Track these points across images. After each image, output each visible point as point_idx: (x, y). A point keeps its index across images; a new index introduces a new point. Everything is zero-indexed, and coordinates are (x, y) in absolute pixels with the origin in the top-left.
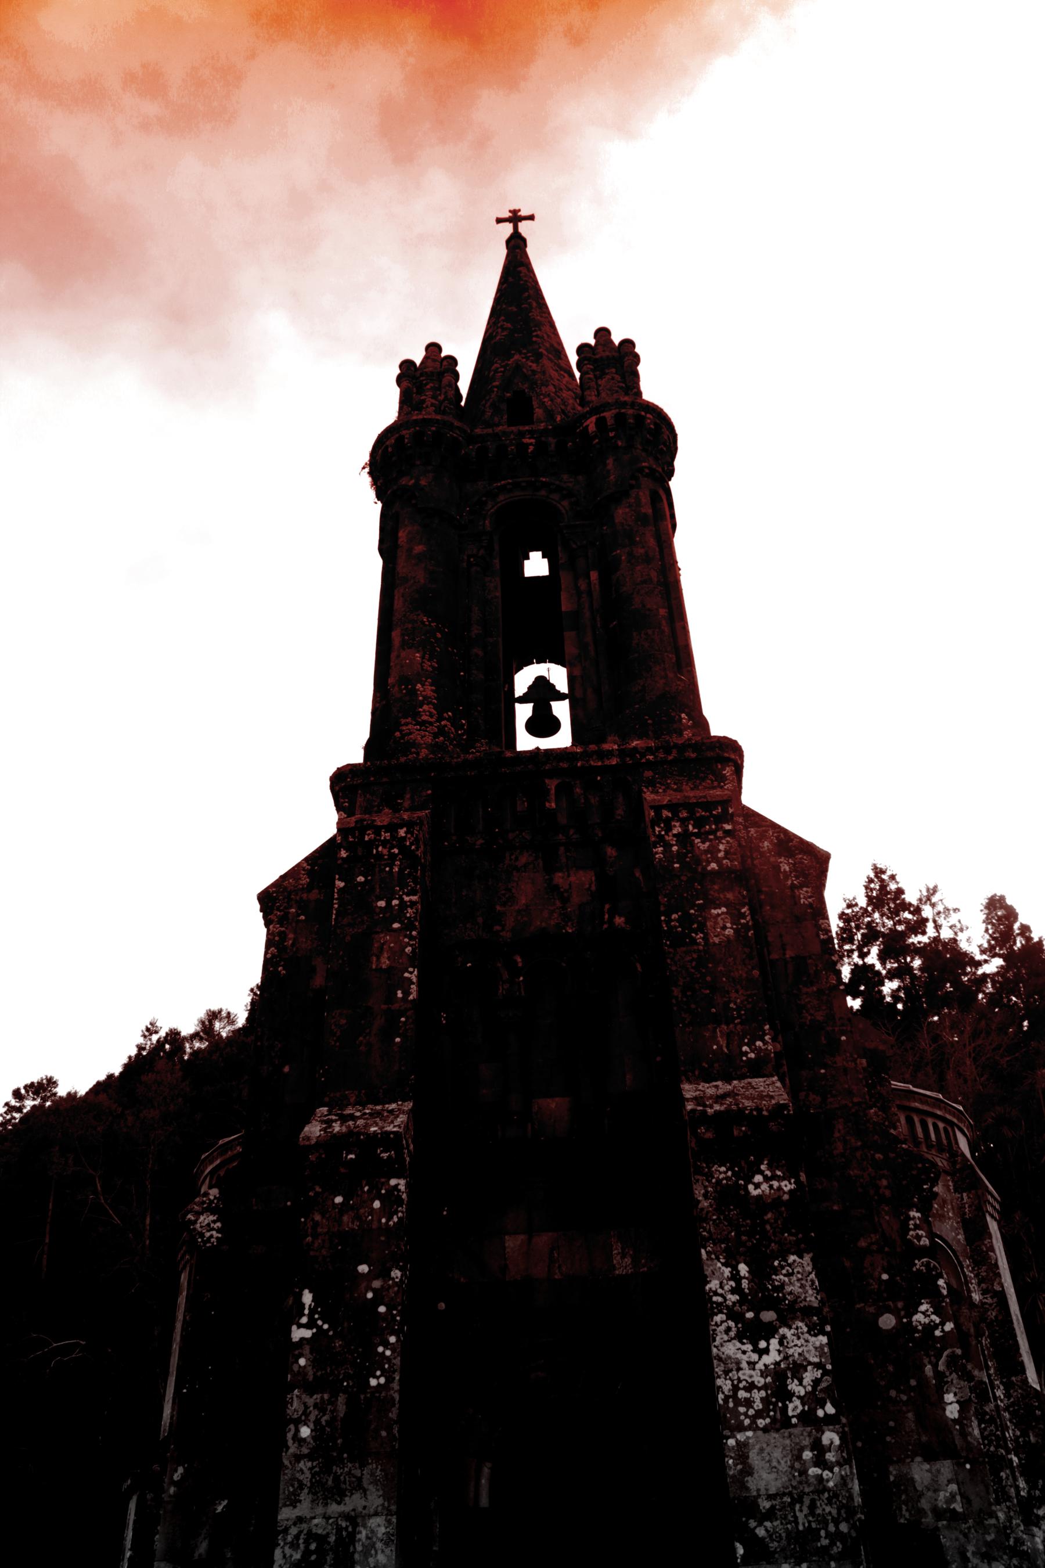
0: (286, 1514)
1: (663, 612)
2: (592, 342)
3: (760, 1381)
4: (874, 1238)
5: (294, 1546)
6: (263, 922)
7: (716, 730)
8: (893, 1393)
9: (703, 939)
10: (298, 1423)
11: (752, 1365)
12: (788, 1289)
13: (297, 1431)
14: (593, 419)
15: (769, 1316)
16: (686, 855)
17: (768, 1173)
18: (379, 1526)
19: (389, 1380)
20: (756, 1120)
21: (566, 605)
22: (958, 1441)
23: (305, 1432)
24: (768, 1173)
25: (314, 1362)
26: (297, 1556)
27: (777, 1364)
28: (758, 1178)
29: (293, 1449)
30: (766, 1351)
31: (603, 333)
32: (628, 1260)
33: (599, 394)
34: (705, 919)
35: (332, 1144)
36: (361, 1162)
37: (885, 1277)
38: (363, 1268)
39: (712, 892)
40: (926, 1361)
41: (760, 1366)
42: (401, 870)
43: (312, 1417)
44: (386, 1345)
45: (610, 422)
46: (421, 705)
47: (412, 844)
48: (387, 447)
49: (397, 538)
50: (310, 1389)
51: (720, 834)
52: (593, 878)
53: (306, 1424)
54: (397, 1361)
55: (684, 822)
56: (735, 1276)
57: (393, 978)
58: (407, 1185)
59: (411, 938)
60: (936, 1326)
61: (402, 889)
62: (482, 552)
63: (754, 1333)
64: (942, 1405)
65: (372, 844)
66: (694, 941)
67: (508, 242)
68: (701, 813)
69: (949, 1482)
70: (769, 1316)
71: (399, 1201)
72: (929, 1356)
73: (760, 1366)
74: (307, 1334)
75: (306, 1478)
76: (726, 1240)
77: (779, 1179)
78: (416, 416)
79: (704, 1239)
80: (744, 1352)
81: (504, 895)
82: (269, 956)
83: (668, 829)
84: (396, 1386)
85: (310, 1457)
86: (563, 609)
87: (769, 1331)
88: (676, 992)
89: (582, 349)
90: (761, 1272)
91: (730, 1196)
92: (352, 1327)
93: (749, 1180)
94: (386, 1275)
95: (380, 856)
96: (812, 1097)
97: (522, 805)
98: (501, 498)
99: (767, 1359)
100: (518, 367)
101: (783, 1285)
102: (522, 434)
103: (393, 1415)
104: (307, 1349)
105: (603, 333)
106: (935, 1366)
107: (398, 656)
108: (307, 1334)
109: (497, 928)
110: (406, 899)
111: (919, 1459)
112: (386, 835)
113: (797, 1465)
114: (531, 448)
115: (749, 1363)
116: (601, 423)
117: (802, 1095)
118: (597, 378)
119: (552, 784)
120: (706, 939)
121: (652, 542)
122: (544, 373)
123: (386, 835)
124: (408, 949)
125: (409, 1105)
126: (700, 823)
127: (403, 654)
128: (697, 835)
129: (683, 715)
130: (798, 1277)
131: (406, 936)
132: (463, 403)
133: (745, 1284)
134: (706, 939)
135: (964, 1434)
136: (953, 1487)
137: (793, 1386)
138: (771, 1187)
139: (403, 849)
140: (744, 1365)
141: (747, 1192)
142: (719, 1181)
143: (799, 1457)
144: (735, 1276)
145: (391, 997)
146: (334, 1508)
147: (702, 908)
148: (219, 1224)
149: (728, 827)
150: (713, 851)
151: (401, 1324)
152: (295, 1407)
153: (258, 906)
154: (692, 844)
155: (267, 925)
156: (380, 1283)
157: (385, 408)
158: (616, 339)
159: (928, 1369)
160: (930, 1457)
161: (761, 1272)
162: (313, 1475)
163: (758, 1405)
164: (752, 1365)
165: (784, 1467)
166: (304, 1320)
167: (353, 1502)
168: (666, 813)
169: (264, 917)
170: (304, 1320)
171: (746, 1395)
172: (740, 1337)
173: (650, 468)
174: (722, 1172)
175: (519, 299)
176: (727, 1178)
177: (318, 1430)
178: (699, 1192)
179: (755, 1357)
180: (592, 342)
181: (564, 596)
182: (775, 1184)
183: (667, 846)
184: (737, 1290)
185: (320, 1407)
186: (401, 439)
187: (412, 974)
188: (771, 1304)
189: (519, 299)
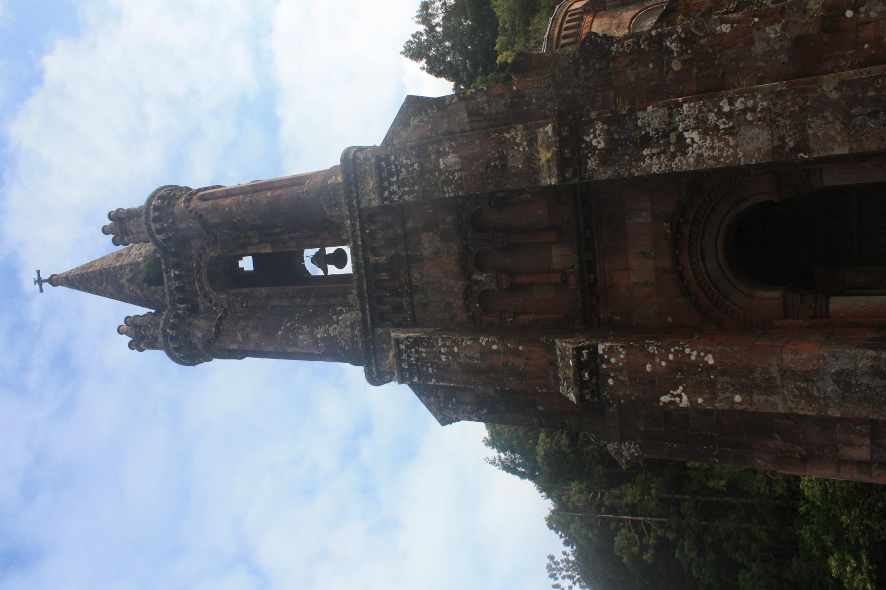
1: (269, 194)
2: (111, 236)
3: (708, 143)
4: (628, 72)
7: (338, 162)
10: (733, 403)
11: (700, 148)
12: (657, 125)
13: (737, 403)
15: (673, 137)
16: (410, 183)
17: (592, 136)
19: (710, 352)
20: (562, 143)
21: (267, 250)
23: (738, 398)
24: (592, 136)
25: (701, 396)
27: (699, 133)
28: (594, 143)
30: (692, 139)
31: (105, 231)
32: (643, 214)
33: (143, 232)
34: (447, 171)
35: (581, 385)
38: (648, 367)
42: (424, 347)
43: (731, 395)
44: (690, 355)
45: (158, 226)
46: (329, 334)
49: (233, 350)
51: (397, 163)
53: (733, 398)
54: (700, 348)
55: (391, 184)
58: (602, 342)
61: (434, 346)
62: (239, 299)
64: (723, 34)
65: (409, 364)
66: (460, 178)
67: (54, 286)
68: (385, 175)
70: (673, 137)
71: (611, 348)
74: (685, 398)
75: (762, 398)
76: (630, 161)
77: (595, 130)
78: (161, 339)
79: (630, 173)
80: (693, 152)
83: (394, 193)
84: (713, 349)
87: (681, 138)
89: (115, 242)
91: (605, 157)
92: (683, 372)
93: (596, 148)
96: (549, 107)
97: (384, 275)
98: (207, 289)
99: (697, 139)
100: (129, 280)
102: (169, 278)
103: (729, 350)
105: (105, 231)
106: (701, 37)
108: (685, 398)
110: (440, 344)
111: (753, 48)
112: (405, 356)
113: (755, 123)
114: (177, 272)
116: (159, 231)
117: (548, 113)
118: (132, 234)
119: (373, 259)
120: (458, 171)
121: (228, 201)
122: (131, 264)
123: (405, 356)
124: (468, 342)
125: (558, 342)
126: (391, 174)
127: (301, 345)
128: (398, 176)
130: (652, 117)
132: (153, 311)
133: (655, 151)
134: (458, 171)
135: (739, 22)
138: (599, 135)
140: (700, 152)
142: (597, 165)
143: (751, 122)
145: (497, 352)
147: (441, 172)
148: (627, 443)
149: (393, 158)
150: (406, 166)
151: (679, 346)
153: (448, 426)
154: (403, 179)
155: (459, 421)
157: (157, 357)
158: (109, 222)
160: (752, 43)
161: (646, 141)
162: (761, 394)
163: (722, 144)
164: (700, 148)
165: (756, 130)
166: (677, 399)
170: (677, 399)
171: (717, 151)
172: (684, 154)
173: (185, 202)
174: (591, 164)
175: (88, 280)
176: (595, 159)
178: (603, 177)
180: (111, 236)
181: (263, 251)
182: (598, 132)
183: (405, 193)
184: (658, 155)
185: (725, 390)
186: (175, 348)
187: (483, 340)
188: (666, 135)
189: (88, 280)
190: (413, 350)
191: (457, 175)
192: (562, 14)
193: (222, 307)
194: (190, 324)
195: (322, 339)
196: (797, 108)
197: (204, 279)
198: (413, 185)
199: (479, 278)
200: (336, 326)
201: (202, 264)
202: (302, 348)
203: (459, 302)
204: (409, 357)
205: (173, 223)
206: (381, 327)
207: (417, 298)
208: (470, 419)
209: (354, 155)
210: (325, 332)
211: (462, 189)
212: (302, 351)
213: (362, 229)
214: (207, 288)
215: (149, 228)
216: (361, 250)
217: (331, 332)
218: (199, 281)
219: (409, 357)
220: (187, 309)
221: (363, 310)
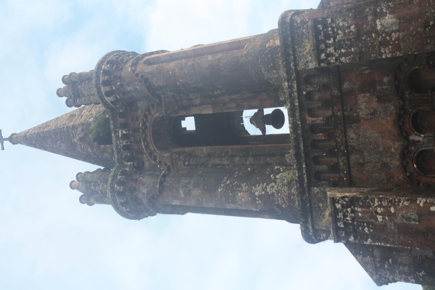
1: (210, 58)
2: (65, 98)
6: (393, 284)
7: (275, 26)
9: (395, 33)
14: (106, 98)
16: (346, 45)
21: (208, 111)
31: (60, 93)
33: (93, 95)
34: (384, 32)
39: (368, 29)
42: (360, 207)
45: (107, 89)
46: (266, 192)
48: (127, 211)
49: (176, 206)
51: (334, 25)
52: (362, 95)
55: (327, 46)
59: (399, 201)
61: (370, 206)
62: (182, 157)
65: (345, 224)
66: (398, 39)
67: (14, 144)
68: (321, 37)
78: (109, 195)
81: (373, 146)
82: (413, 280)
86: (211, 112)
89: (69, 104)
97: (320, 136)
98: (152, 148)
100: (81, 139)
102: (117, 138)
105: (60, 93)
110: (376, 204)
112: (340, 215)
114: (124, 132)
116: (108, 94)
118: (84, 96)
119: (309, 120)
120: (395, 32)
121: (172, 64)
122: (83, 124)
123: (340, 215)
124: (406, 203)
126: (327, 37)
127: (239, 202)
128: (335, 38)
131: (399, 205)
132: (102, 168)
134: (395, 32)
147: (378, 34)
149: (329, 21)
150: (342, 28)
153: (384, 286)
154: (340, 41)
155: (395, 281)
157: (106, 212)
158: (63, 86)
168: (323, 56)
169: (391, 282)
173: (131, 66)
175: (44, 139)
180: (65, 98)
181: (204, 112)
183: (342, 55)
186: (122, 204)
189: (44, 139)
190: (349, 210)
191: (394, 36)
193: (165, 164)
194: (136, 181)
195: (260, 197)
197: (150, 139)
198: (350, 47)
199: (417, 138)
200: (273, 184)
201: (148, 125)
202: (241, 205)
203: (396, 163)
204: (345, 216)
205: (121, 85)
206: (318, 186)
207: (353, 158)
208: (407, 281)
209: (291, 19)
210: (263, 190)
211: (400, 50)
212: (240, 208)
213: (299, 91)
214: (152, 147)
215: (99, 91)
216: (297, 111)
217: (268, 190)
218: (145, 140)
219: (345, 216)
220: (134, 167)
221: (300, 169)
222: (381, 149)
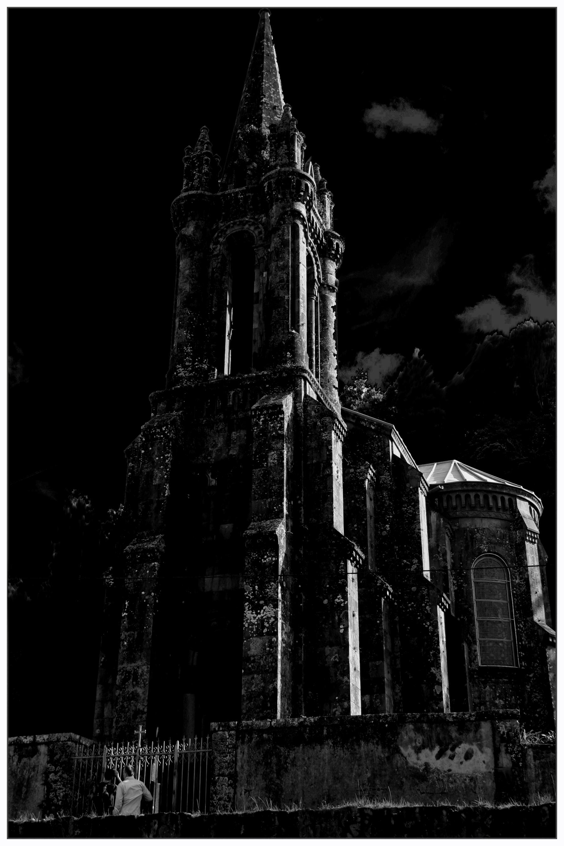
0: (120, 667)
5: (122, 674)
8: (323, 626)
10: (123, 641)
13: (123, 643)
15: (262, 602)
18: (145, 668)
22: (342, 640)
25: (128, 623)
26: (123, 677)
29: (122, 648)
30: (260, 613)
35: (134, 553)
36: (146, 556)
37: (328, 586)
38: (143, 593)
40: (336, 614)
41: (257, 618)
47: (168, 433)
50: (127, 630)
56: (254, 590)
57: (160, 489)
60: (342, 602)
63: (257, 608)
69: (336, 653)
72: (337, 613)
73: (257, 618)
85: (126, 650)
88: (254, 487)
90: (262, 587)
93: (263, 557)
94: (150, 594)
95: (157, 438)
99: (259, 616)
101: (268, 592)
104: (126, 619)
106: (339, 616)
107: (177, 333)
109: (209, 458)
115: (254, 617)
129: (288, 353)
136: (337, 655)
137: (266, 624)
139: (165, 435)
141: (261, 561)
144: (254, 590)
146: (133, 665)
147: (268, 452)
152: (123, 637)
156: (149, 596)
159: (337, 618)
167: (139, 663)
174: (255, 555)
177: (129, 642)
179: (255, 616)
188: (263, 599)
192: (511, 493)
195: (182, 351)
196: (267, 668)
202: (177, 333)
204: (158, 433)
210: (187, 353)
212: (176, 331)
219: (158, 433)
222: (210, 449)
